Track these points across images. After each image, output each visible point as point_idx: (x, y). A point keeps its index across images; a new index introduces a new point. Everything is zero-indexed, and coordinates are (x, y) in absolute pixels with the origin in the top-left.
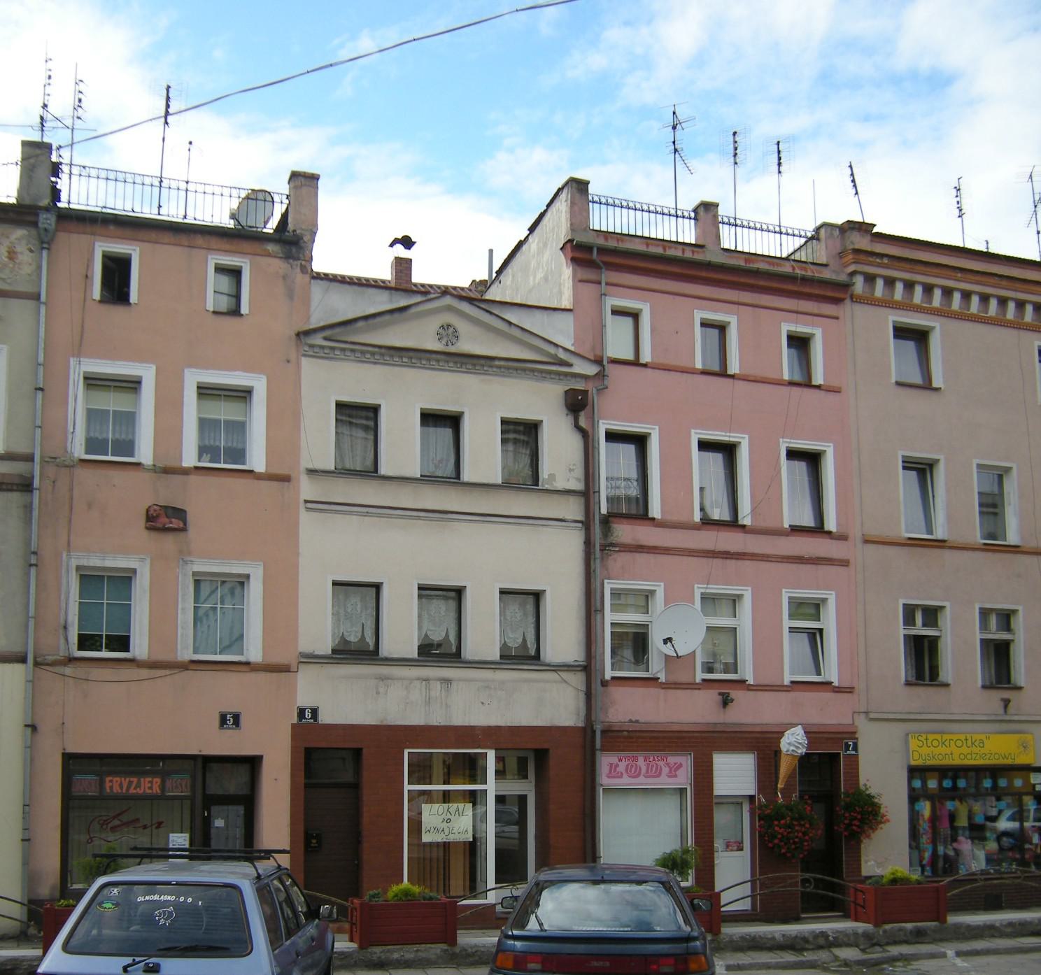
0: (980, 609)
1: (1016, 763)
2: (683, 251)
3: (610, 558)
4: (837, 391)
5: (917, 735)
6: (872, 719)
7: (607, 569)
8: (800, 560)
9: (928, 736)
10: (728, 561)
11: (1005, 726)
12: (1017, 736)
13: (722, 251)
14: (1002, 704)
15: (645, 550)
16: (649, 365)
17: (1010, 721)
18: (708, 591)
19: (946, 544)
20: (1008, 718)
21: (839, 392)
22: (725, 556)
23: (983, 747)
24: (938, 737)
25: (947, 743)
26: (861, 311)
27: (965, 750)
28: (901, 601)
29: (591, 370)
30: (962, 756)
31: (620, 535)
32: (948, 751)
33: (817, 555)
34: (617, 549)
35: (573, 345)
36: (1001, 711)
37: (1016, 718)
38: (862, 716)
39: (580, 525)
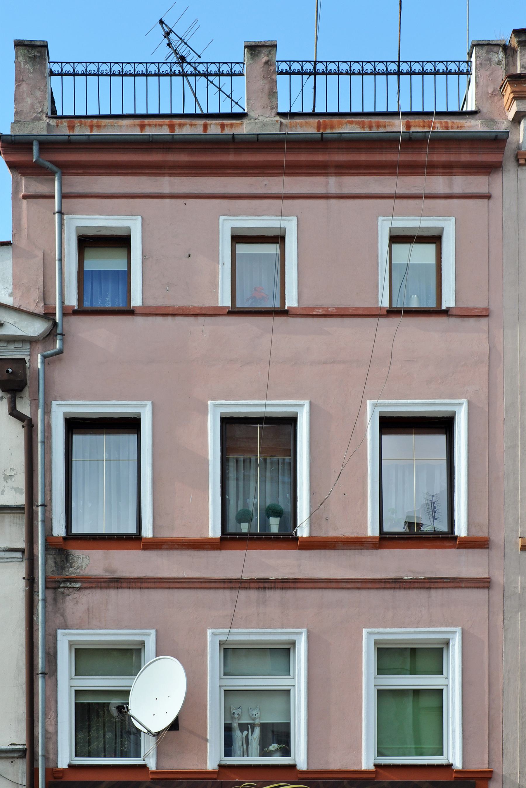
2: (205, 127)
3: (68, 598)
4: (483, 314)
7: (63, 615)
8: (397, 584)
10: (268, 593)
13: (278, 118)
15: (125, 585)
16: (137, 311)
18: (231, 638)
21: (487, 316)
22: (262, 585)
29: (36, 328)
31: (84, 566)
34: (78, 585)
35: (11, 295)
39: (19, 555)
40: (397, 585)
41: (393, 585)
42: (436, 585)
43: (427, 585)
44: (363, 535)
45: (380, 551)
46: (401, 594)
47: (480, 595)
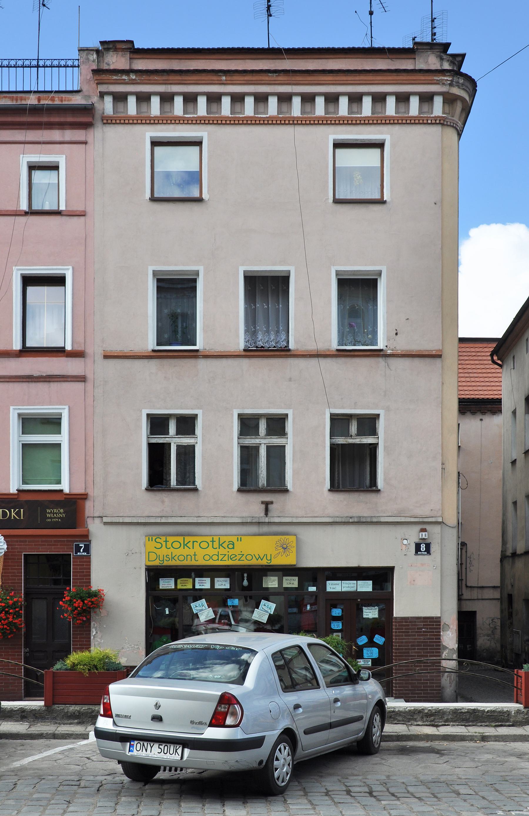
0: (239, 415)
1: (272, 564)
4: (82, 214)
5: (154, 538)
6: (106, 523)
9: (169, 538)
11: (265, 529)
12: (278, 537)
14: (263, 506)
17: (269, 523)
19: (199, 354)
20: (267, 520)
21: (84, 215)
23: (233, 548)
24: (180, 539)
25: (190, 545)
26: (113, 133)
27: (211, 551)
28: (145, 412)
30: (207, 558)
32: (191, 552)
33: (49, 373)
36: (263, 514)
37: (277, 520)
38: (97, 521)
40: (30, 380)
41: (28, 380)
42: (53, 380)
43: (48, 380)
44: (10, 349)
45: (20, 359)
46: (33, 385)
47: (79, 386)
